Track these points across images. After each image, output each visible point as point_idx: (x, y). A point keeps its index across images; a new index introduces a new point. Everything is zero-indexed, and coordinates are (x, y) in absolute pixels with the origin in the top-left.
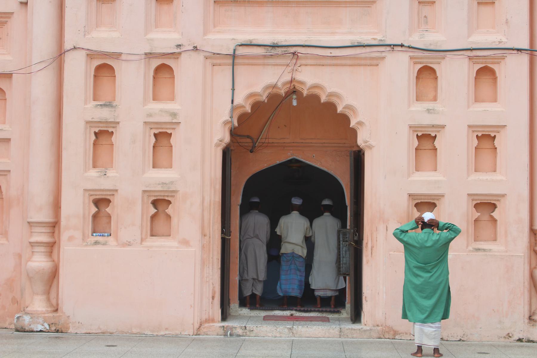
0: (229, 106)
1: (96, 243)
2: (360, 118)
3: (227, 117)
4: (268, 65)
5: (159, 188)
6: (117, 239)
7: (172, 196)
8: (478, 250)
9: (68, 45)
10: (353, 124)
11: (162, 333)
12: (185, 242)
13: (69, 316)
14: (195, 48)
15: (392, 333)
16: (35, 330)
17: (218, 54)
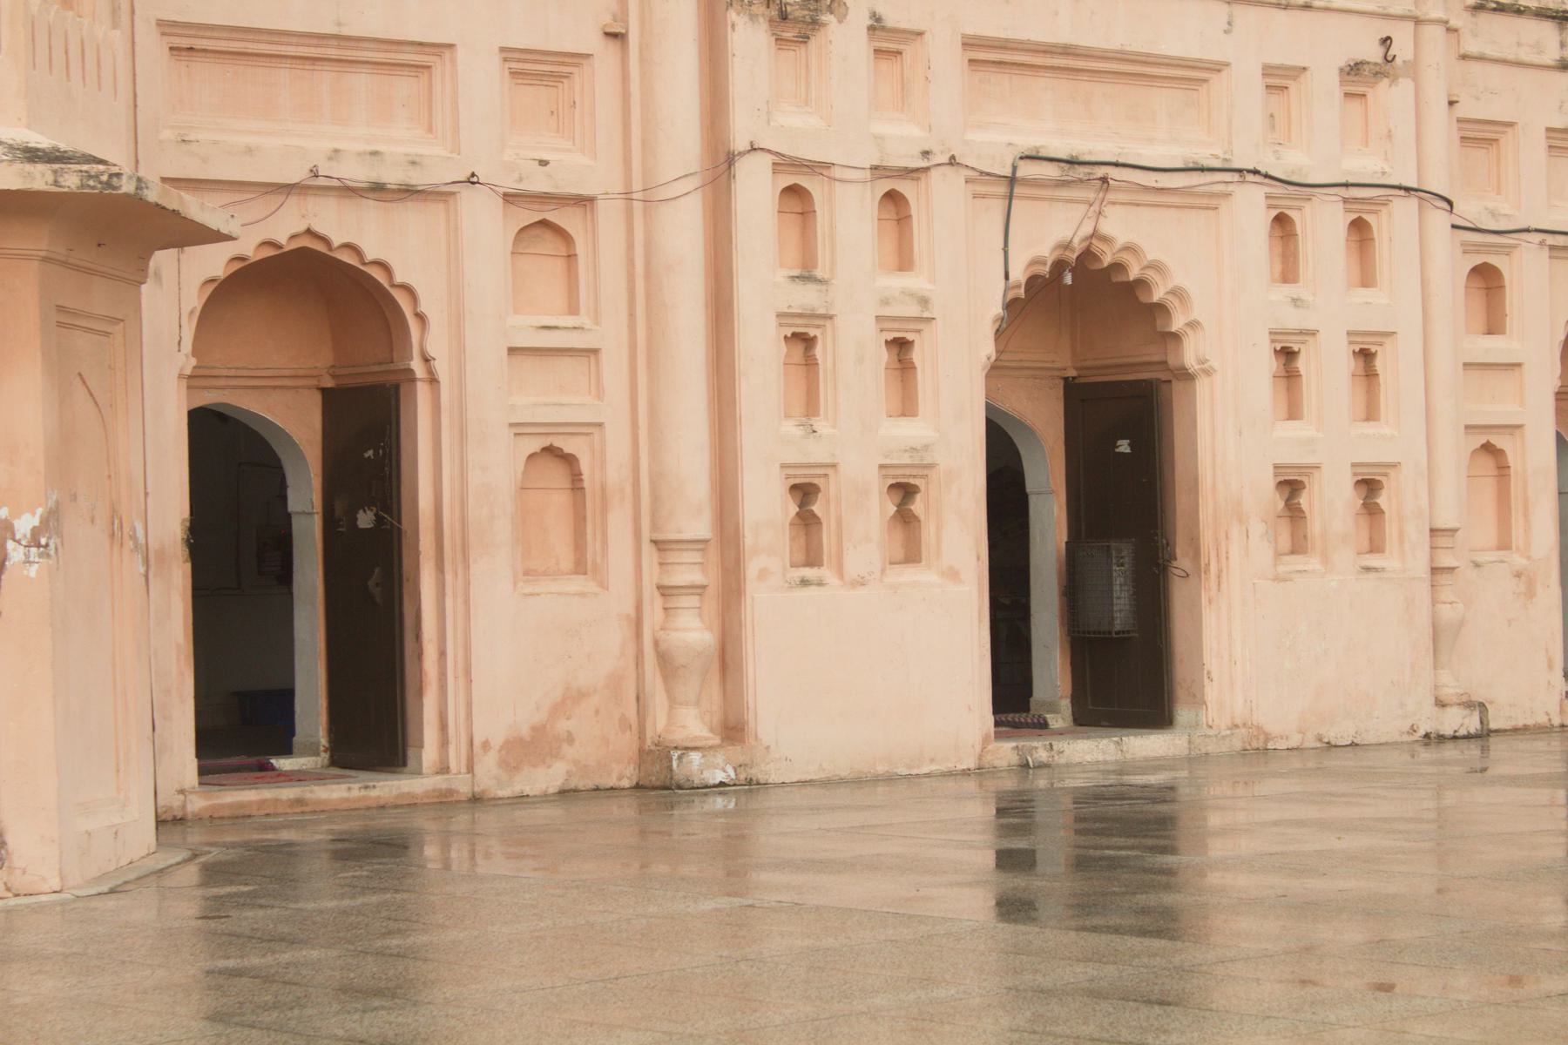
0: (1000, 284)
1: (804, 582)
2: (1196, 314)
3: (997, 309)
4: (1058, 200)
5: (906, 460)
6: (840, 574)
7: (922, 477)
8: (1368, 569)
9: (740, 144)
10: (1177, 324)
11: (925, 770)
12: (953, 575)
13: (768, 748)
14: (953, 161)
15: (1262, 737)
16: (712, 782)
17: (988, 174)
